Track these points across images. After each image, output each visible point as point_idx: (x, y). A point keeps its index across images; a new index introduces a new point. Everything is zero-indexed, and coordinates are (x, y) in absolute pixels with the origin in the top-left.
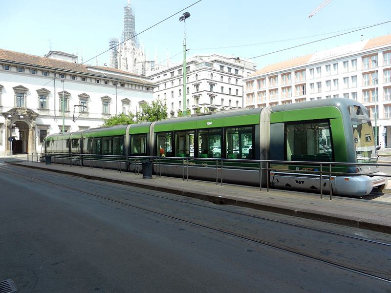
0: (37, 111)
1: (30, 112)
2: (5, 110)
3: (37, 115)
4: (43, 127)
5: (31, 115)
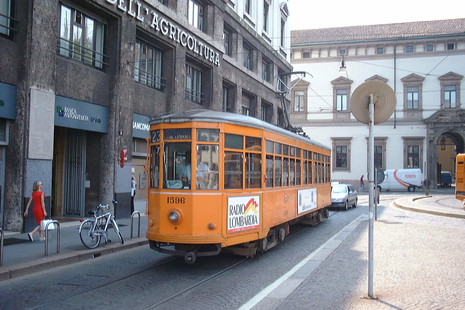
2: (426, 115)
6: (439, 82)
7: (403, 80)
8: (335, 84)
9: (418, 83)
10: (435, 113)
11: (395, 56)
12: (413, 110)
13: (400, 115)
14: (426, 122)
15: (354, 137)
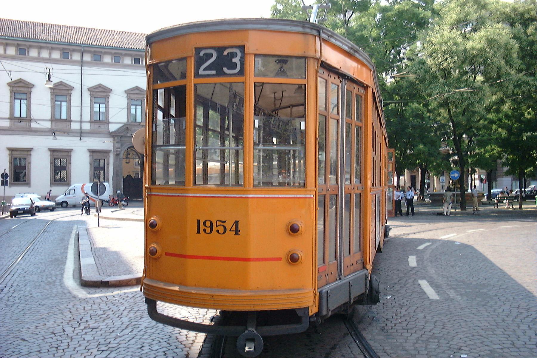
2: (113, 128)
6: (126, 95)
7: (89, 89)
8: (13, 87)
9: (105, 94)
10: (121, 127)
11: (82, 63)
12: (100, 122)
13: (86, 127)
14: (113, 135)
15: (35, 148)
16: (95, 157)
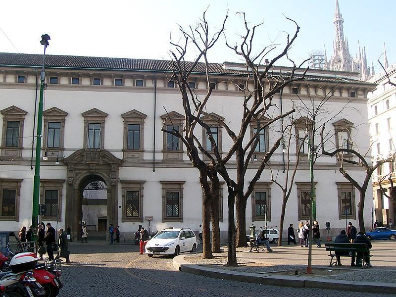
0: (119, 156)
1: (105, 155)
2: (67, 154)
3: (121, 163)
4: (131, 186)
5: (112, 164)
6: (83, 119)
9: (60, 118)
14: (65, 162)
16: (49, 189)
